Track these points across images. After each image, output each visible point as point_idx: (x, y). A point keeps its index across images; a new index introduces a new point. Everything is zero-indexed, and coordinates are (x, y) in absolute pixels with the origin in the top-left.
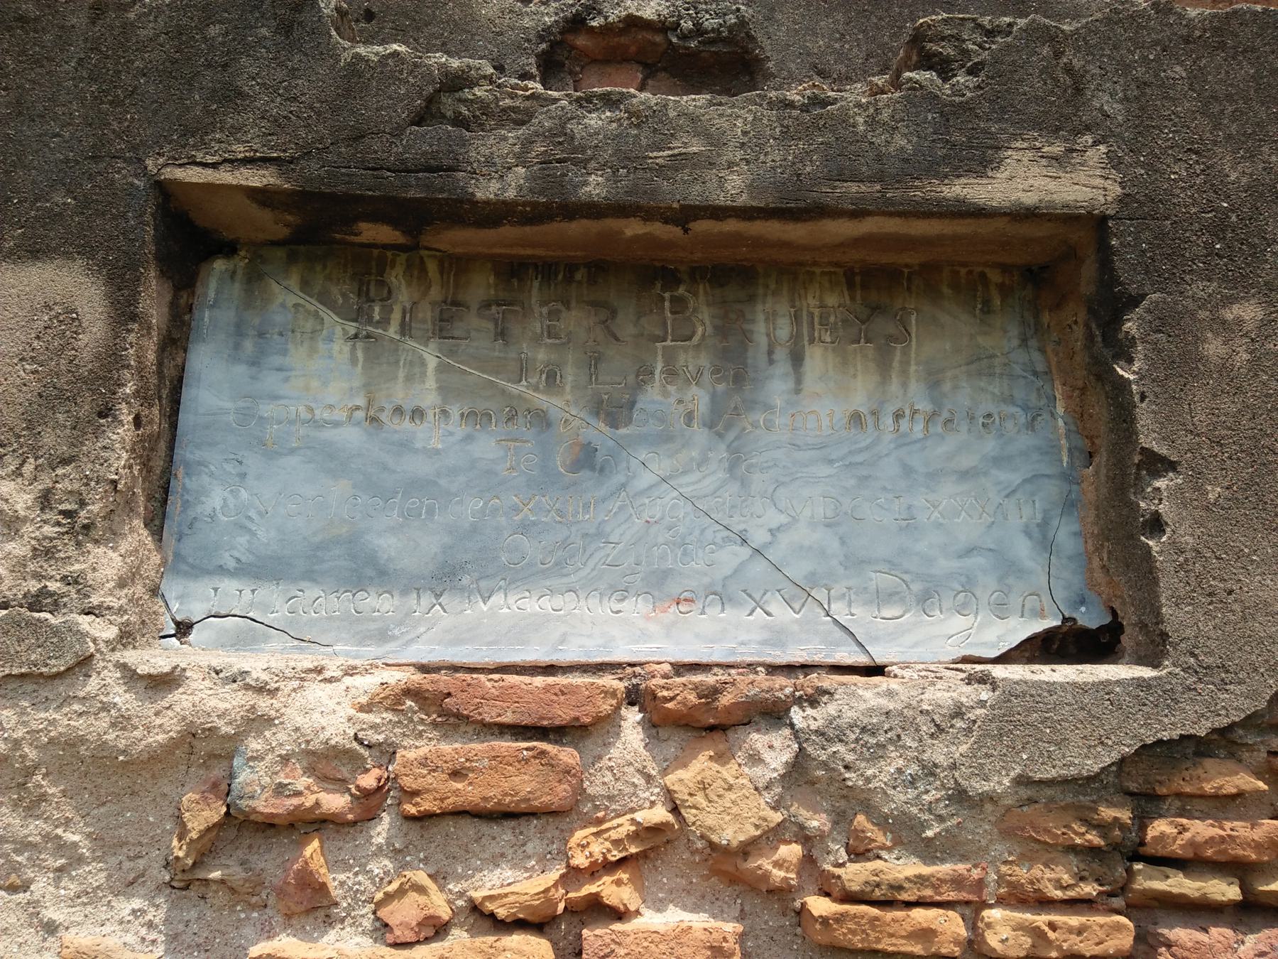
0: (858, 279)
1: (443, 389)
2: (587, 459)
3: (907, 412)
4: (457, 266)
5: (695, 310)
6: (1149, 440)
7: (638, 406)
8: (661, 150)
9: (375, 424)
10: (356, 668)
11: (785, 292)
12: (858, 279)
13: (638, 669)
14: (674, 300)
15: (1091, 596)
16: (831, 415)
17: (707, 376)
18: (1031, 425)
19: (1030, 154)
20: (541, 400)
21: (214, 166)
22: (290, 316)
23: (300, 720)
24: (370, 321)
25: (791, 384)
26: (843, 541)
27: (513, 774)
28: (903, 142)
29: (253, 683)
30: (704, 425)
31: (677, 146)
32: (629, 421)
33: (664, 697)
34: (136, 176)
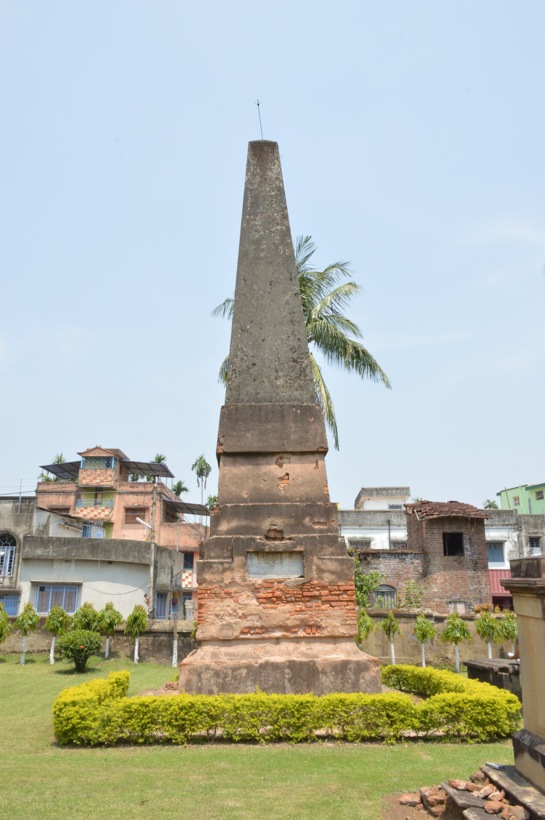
2: (272, 566)
27: (270, 585)
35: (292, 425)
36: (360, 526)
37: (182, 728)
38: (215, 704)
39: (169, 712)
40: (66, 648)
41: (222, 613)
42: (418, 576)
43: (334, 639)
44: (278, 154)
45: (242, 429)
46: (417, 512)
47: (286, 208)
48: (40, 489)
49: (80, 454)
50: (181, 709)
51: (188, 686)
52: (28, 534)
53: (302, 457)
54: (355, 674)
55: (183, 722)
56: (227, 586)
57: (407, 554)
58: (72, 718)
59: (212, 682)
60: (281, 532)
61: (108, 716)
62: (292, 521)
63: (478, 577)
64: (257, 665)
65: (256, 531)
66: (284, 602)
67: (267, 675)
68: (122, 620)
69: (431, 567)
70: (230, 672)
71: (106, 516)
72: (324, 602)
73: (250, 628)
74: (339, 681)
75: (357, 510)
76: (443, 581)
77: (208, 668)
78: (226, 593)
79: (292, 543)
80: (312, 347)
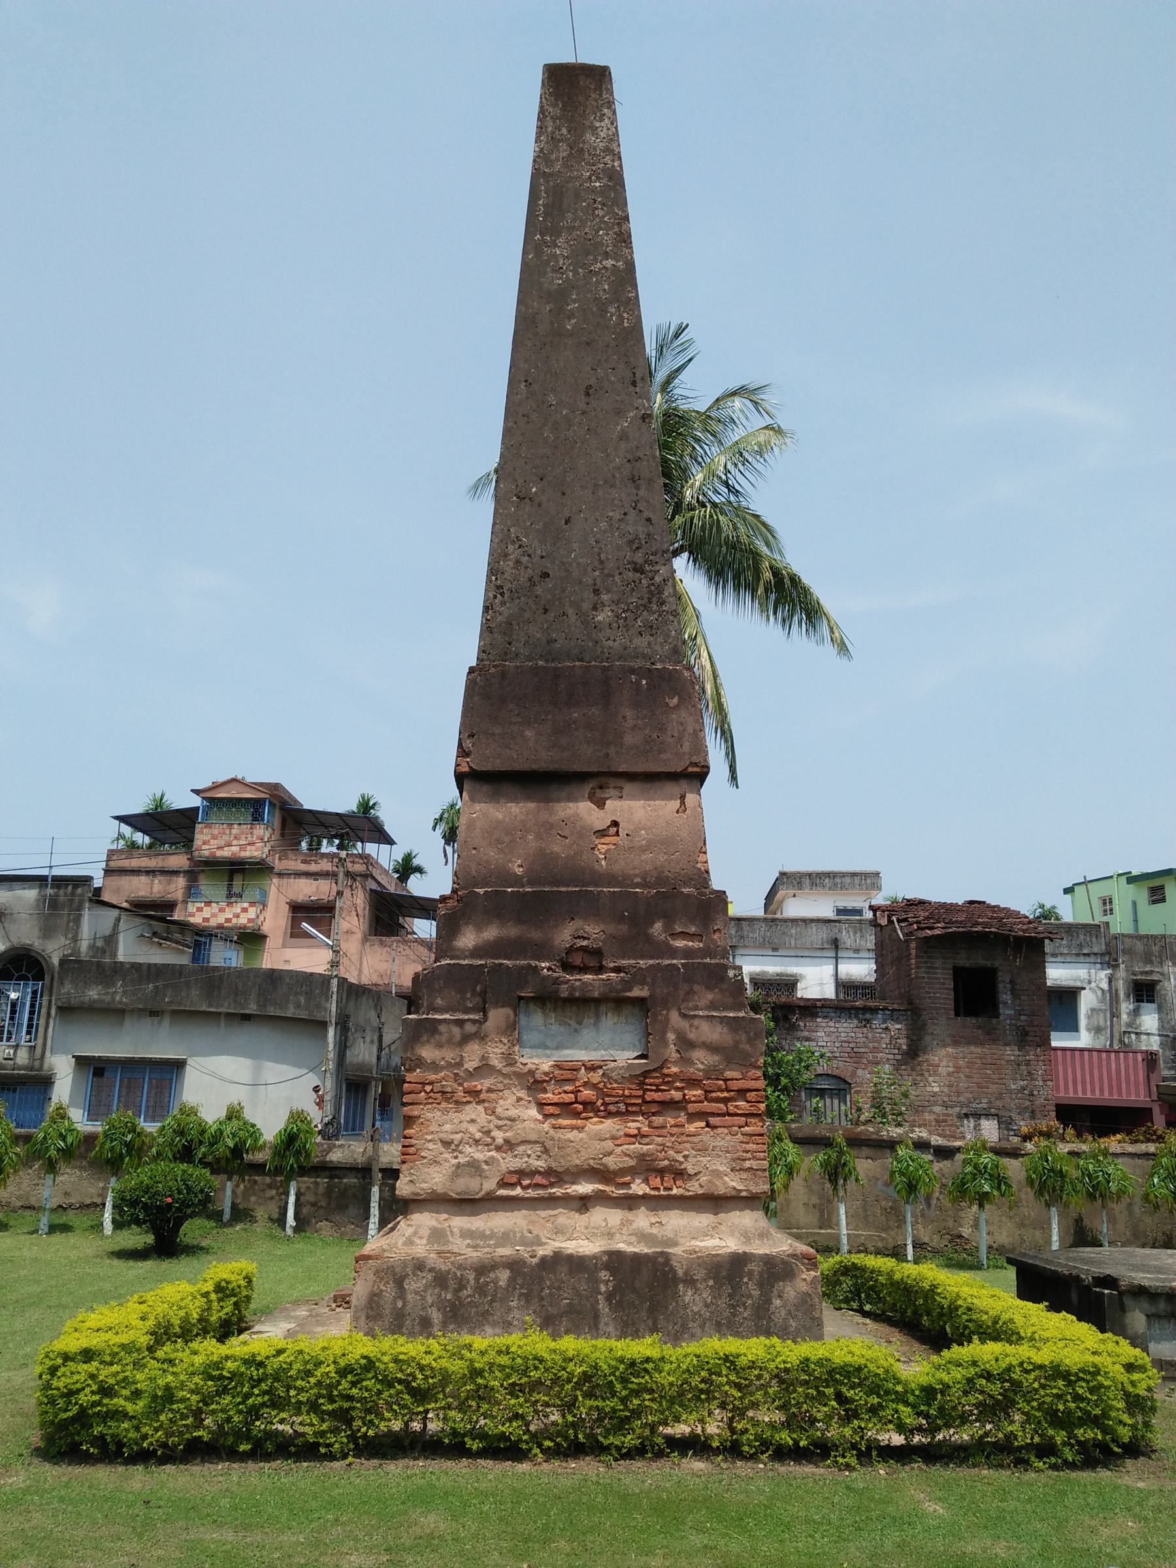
2: (576, 1031)
27: (568, 1075)
35: (629, 713)
36: (775, 949)
37: (343, 1417)
38: (423, 1362)
39: (312, 1380)
40: (134, 1203)
41: (458, 1137)
42: (899, 1057)
43: (714, 1202)
44: (612, 94)
45: (514, 719)
46: (899, 921)
47: (627, 218)
48: (112, 864)
49: (197, 792)
50: (343, 1372)
51: (372, 1308)
52: (71, 955)
53: (649, 785)
54: (761, 1285)
55: (346, 1405)
56: (471, 1075)
57: (874, 1011)
58: (78, 1391)
59: (430, 1300)
60: (597, 953)
61: (167, 1388)
62: (624, 928)
63: (1028, 1063)
64: (534, 1261)
65: (541, 950)
66: (602, 1114)
67: (556, 1285)
68: (261, 1142)
69: (928, 1038)
70: (472, 1277)
71: (250, 920)
72: (692, 1117)
73: (521, 1173)
74: (723, 1303)
75: (769, 916)
76: (950, 1069)
77: (420, 1266)
78: (468, 1092)
79: (622, 979)
80: (682, 565)
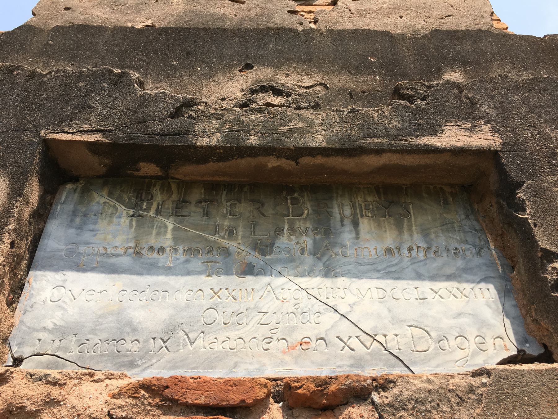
0: (381, 190)
1: (175, 239)
3: (414, 248)
4: (186, 186)
5: (303, 203)
6: (544, 244)
7: (276, 245)
8: (284, 126)
9: (138, 255)
10: (113, 375)
11: (347, 196)
12: (381, 190)
13: (279, 382)
14: (291, 199)
15: (530, 338)
16: (376, 249)
17: (311, 232)
18: (479, 253)
19: (455, 128)
20: (226, 243)
21: (73, 133)
22: (101, 207)
23: (76, 402)
24: (141, 209)
25: (354, 235)
26: (390, 311)
28: (396, 123)
29: (51, 380)
30: (311, 254)
31: (292, 125)
32: (271, 253)
33: (296, 386)
34: (34, 138)
